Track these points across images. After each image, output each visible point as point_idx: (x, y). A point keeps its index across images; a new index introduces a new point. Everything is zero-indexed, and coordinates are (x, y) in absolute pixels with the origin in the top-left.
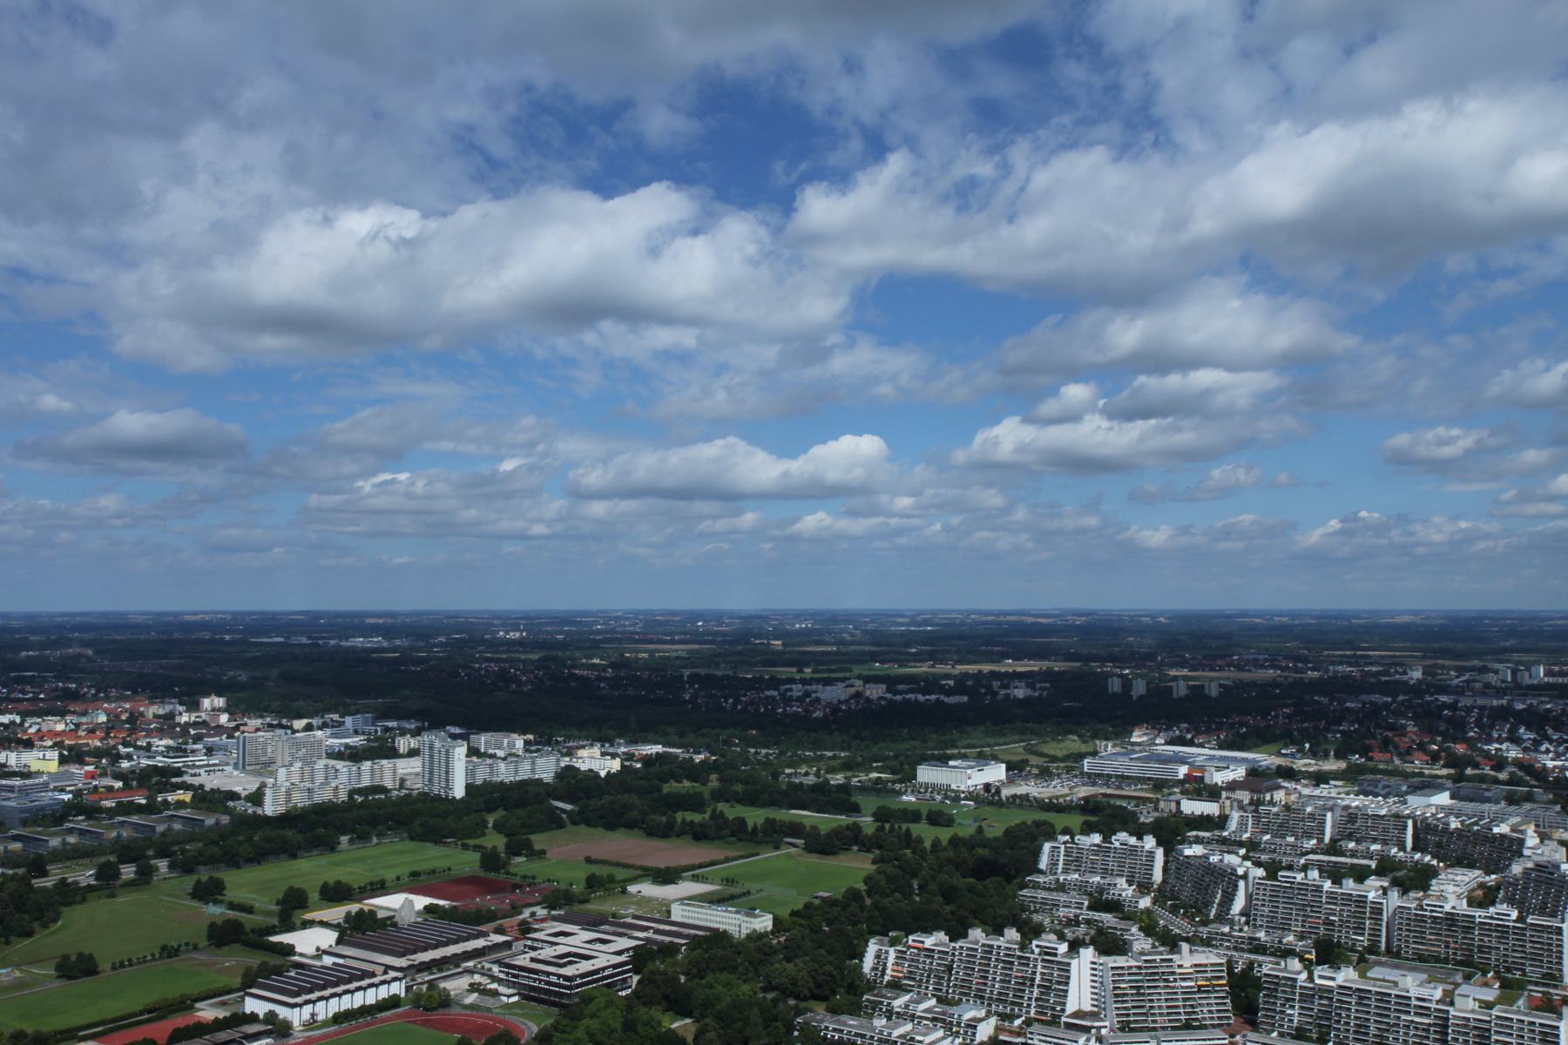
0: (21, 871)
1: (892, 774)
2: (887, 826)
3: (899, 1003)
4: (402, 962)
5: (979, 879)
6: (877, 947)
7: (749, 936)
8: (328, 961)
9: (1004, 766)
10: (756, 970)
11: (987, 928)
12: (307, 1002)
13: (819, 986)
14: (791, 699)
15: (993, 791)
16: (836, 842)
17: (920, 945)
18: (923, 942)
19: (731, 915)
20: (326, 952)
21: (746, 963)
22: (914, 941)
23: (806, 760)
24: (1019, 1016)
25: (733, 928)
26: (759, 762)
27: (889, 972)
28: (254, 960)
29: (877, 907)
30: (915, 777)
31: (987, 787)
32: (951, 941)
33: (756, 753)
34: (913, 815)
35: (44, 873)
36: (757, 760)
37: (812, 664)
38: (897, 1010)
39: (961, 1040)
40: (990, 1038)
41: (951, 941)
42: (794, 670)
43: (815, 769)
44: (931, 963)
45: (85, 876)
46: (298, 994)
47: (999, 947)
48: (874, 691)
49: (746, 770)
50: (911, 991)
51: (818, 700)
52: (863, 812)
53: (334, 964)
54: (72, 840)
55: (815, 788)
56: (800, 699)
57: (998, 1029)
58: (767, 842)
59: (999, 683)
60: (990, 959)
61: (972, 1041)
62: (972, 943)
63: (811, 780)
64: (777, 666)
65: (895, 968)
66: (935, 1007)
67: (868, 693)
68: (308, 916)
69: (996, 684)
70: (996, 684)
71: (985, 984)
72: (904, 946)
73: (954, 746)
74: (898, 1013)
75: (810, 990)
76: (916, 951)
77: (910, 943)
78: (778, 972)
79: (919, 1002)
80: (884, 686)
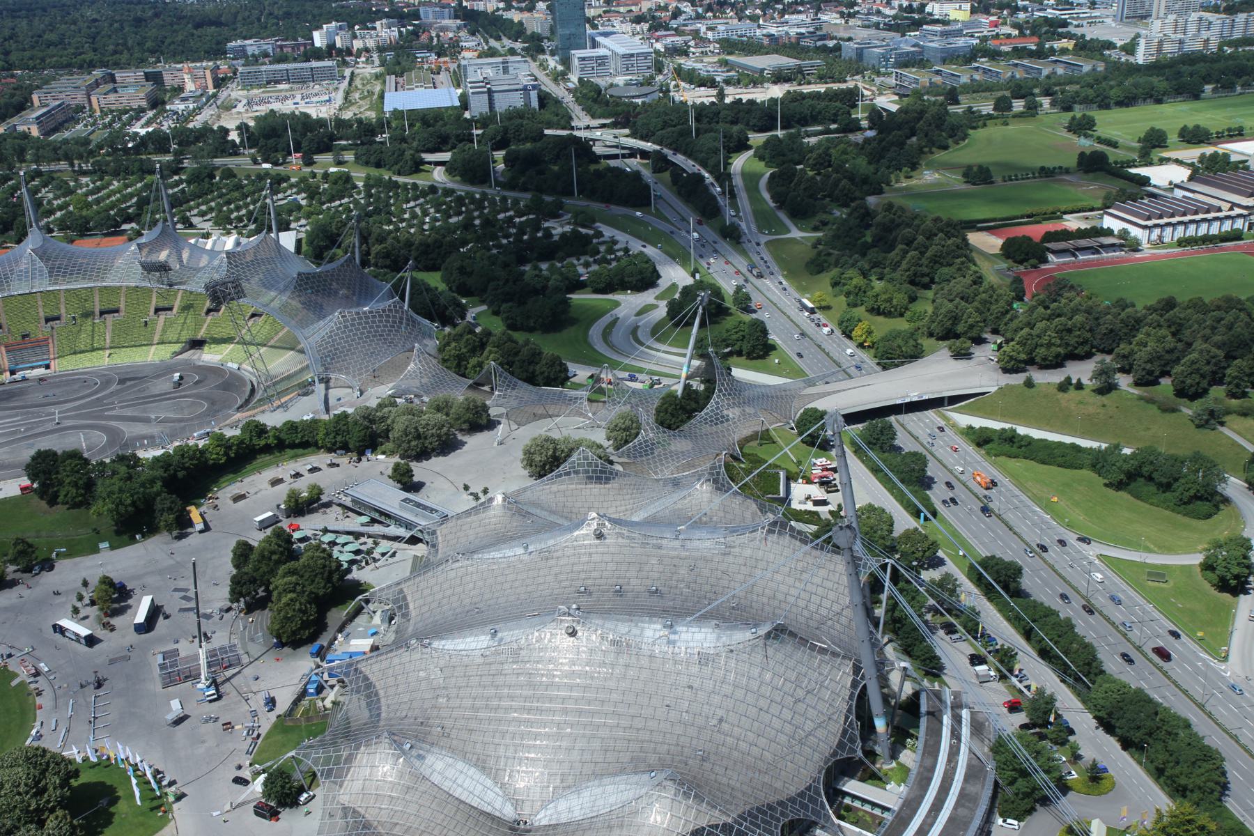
0: (941, 98)
8: (1179, 193)
20: (1177, 186)
28: (1114, 186)
35: (957, 102)
45: (987, 108)
46: (1149, 218)
53: (1184, 197)
54: (977, 77)
68: (1165, 154)
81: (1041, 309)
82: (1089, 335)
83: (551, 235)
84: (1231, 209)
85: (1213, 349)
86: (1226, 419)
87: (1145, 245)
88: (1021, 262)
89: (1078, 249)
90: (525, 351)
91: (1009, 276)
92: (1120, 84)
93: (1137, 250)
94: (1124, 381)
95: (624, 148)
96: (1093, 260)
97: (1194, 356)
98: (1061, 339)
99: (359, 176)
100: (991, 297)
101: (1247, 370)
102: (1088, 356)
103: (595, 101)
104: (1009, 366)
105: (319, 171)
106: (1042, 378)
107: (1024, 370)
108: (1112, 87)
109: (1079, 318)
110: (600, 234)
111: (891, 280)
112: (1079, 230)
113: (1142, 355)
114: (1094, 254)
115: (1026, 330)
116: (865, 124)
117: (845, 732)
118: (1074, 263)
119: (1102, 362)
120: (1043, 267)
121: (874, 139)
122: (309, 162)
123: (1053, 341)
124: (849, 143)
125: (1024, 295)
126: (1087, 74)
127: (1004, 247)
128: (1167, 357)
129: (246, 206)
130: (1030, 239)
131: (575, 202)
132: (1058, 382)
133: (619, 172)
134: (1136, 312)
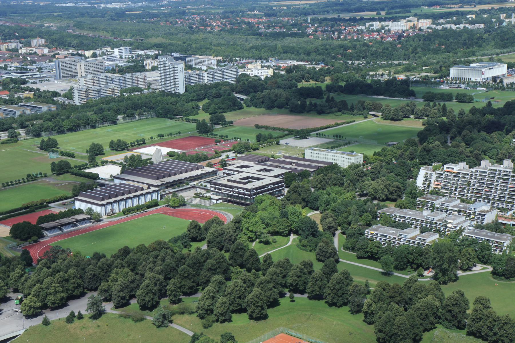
1: (435, 73)
2: (432, 104)
3: (438, 203)
4: (158, 182)
5: (488, 133)
6: (425, 172)
7: (350, 167)
8: (117, 182)
9: (506, 66)
10: (354, 185)
11: (492, 160)
12: (108, 203)
13: (391, 193)
14: (373, 31)
15: (498, 81)
16: (401, 113)
17: (451, 170)
18: (453, 168)
19: (339, 155)
20: (115, 177)
21: (349, 181)
22: (447, 168)
23: (382, 67)
24: (511, 210)
25: (341, 162)
26: (354, 69)
27: (432, 185)
29: (425, 149)
30: (449, 75)
31: (494, 79)
32: (470, 168)
33: (352, 63)
34: (448, 97)
36: (352, 67)
37: (386, 9)
38: (437, 206)
39: (475, 222)
40: (493, 222)
41: (470, 168)
42: (375, 13)
43: (387, 72)
44: (458, 180)
46: (103, 199)
47: (500, 171)
48: (425, 24)
49: (346, 74)
50: (445, 196)
51: (389, 30)
52: (417, 95)
53: (121, 184)
55: (388, 82)
56: (378, 31)
57: (497, 216)
58: (360, 114)
59: (505, 15)
60: (494, 178)
61: (482, 223)
62: (483, 168)
63: (386, 78)
64: (364, 11)
65: (436, 183)
66: (459, 204)
67: (420, 25)
68: (105, 159)
69: (502, 16)
70: (502, 16)
71: (491, 192)
72: (442, 170)
73: (474, 55)
74: (438, 208)
75: (386, 195)
76: (448, 173)
77: (445, 169)
78: (367, 186)
79: (450, 202)
80: (430, 20)
81: (45, 270)
82: (80, 281)
84: (149, 188)
85: (157, 276)
86: (173, 318)
87: (104, 217)
88: (26, 240)
89: (63, 225)
91: (19, 251)
92: (68, 117)
93: (100, 221)
94: (108, 307)
96: (74, 231)
97: (147, 282)
98: (63, 287)
100: (9, 267)
101: (179, 285)
102: (82, 295)
104: (30, 313)
106: (54, 316)
107: (41, 314)
108: (63, 120)
109: (71, 271)
112: (61, 213)
113: (116, 287)
114: (73, 227)
115: (38, 286)
118: (62, 235)
119: (92, 297)
120: (42, 240)
123: (57, 289)
125: (32, 262)
126: (46, 113)
127: (12, 231)
128: (132, 285)
130: (29, 223)
132: (66, 316)
134: (107, 260)
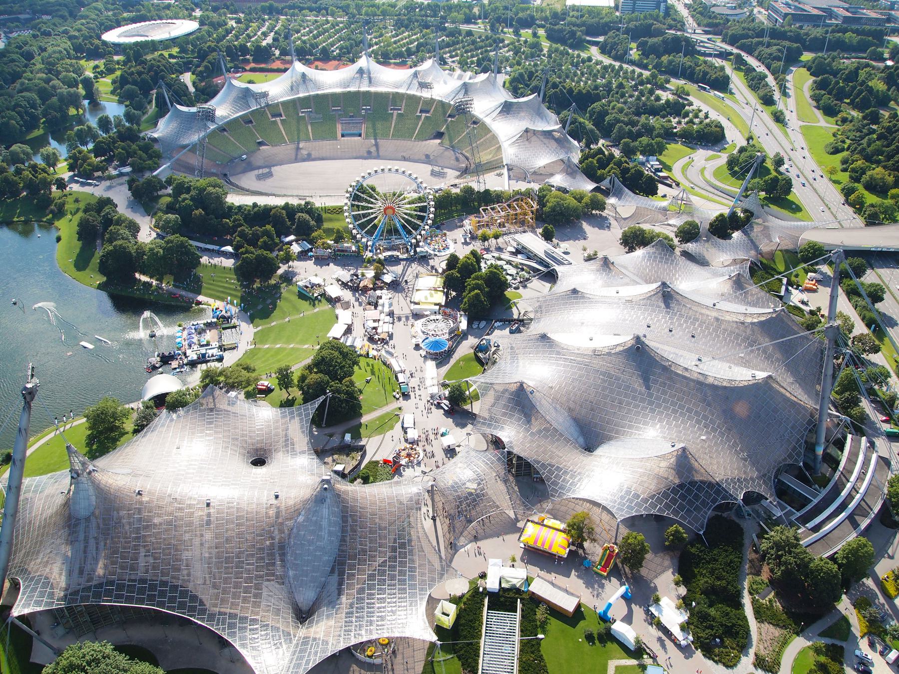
83: (658, 99)
90: (633, 171)
95: (716, 50)
99: (546, 45)
103: (701, 13)
105: (523, 39)
110: (691, 104)
111: (885, 167)
116: (886, 56)
117: (794, 449)
121: (892, 67)
122: (517, 33)
124: (874, 68)
129: (477, 55)
131: (676, 83)
133: (712, 66)
